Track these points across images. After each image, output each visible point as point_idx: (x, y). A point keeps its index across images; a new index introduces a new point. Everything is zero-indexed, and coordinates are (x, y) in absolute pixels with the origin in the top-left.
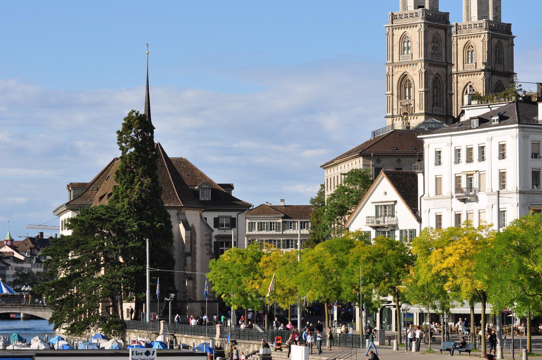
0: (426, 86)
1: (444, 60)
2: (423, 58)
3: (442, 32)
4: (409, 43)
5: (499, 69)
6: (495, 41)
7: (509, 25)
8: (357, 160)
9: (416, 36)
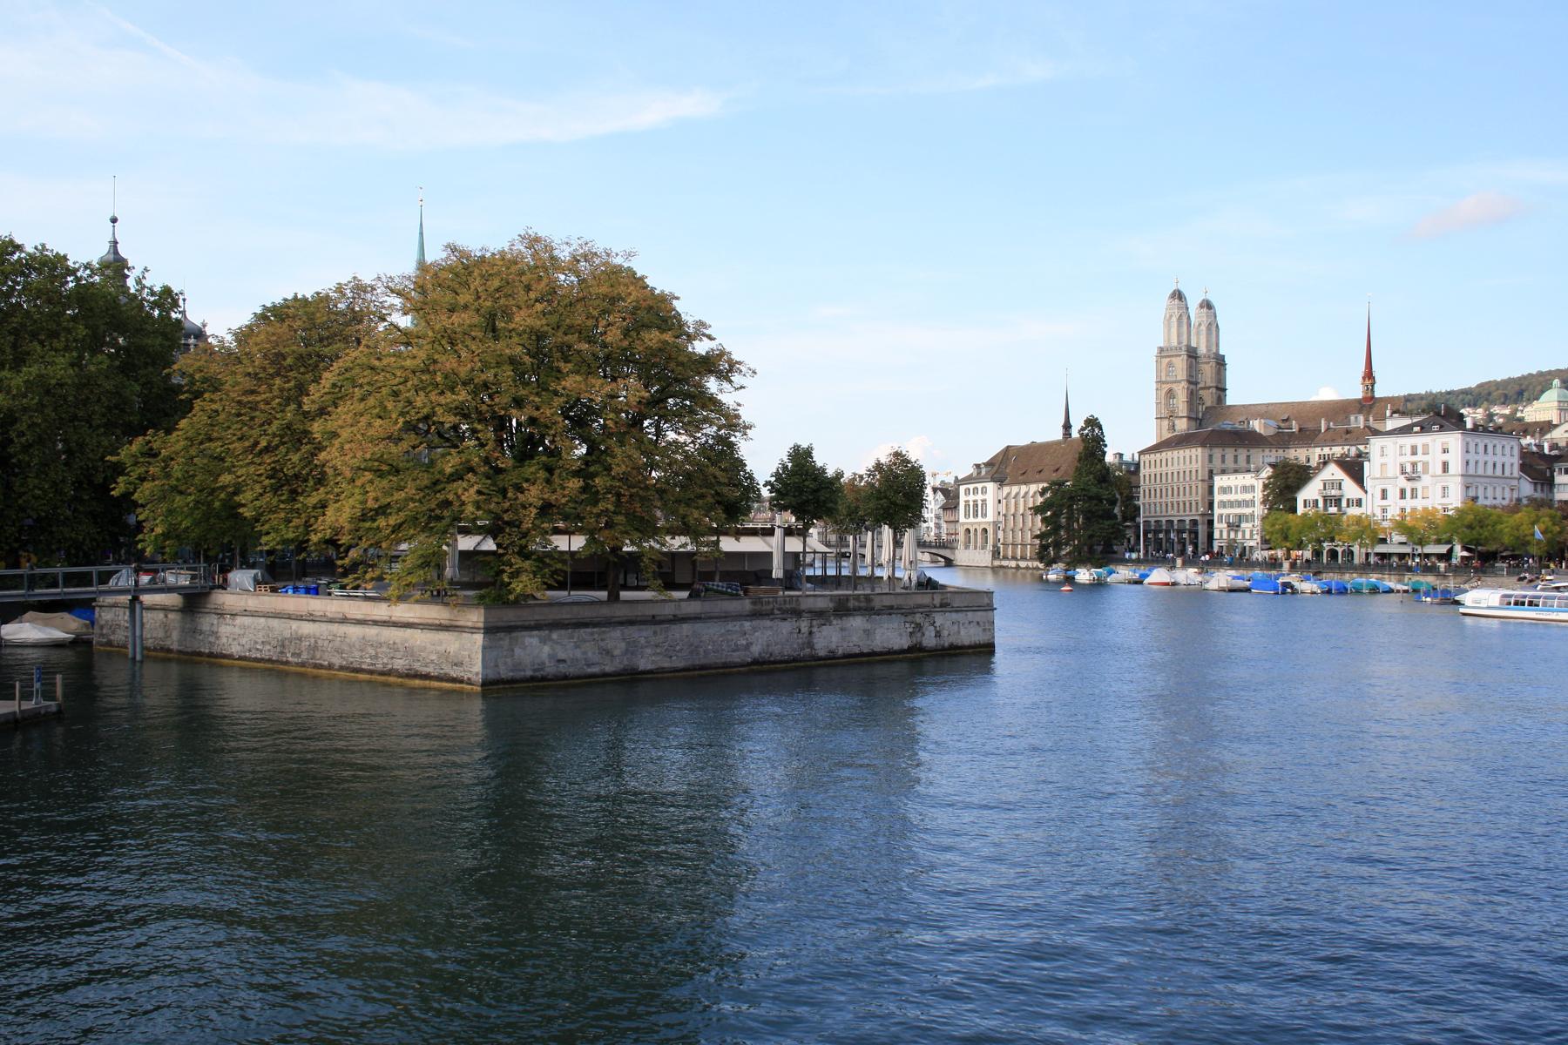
9: (1181, 364)
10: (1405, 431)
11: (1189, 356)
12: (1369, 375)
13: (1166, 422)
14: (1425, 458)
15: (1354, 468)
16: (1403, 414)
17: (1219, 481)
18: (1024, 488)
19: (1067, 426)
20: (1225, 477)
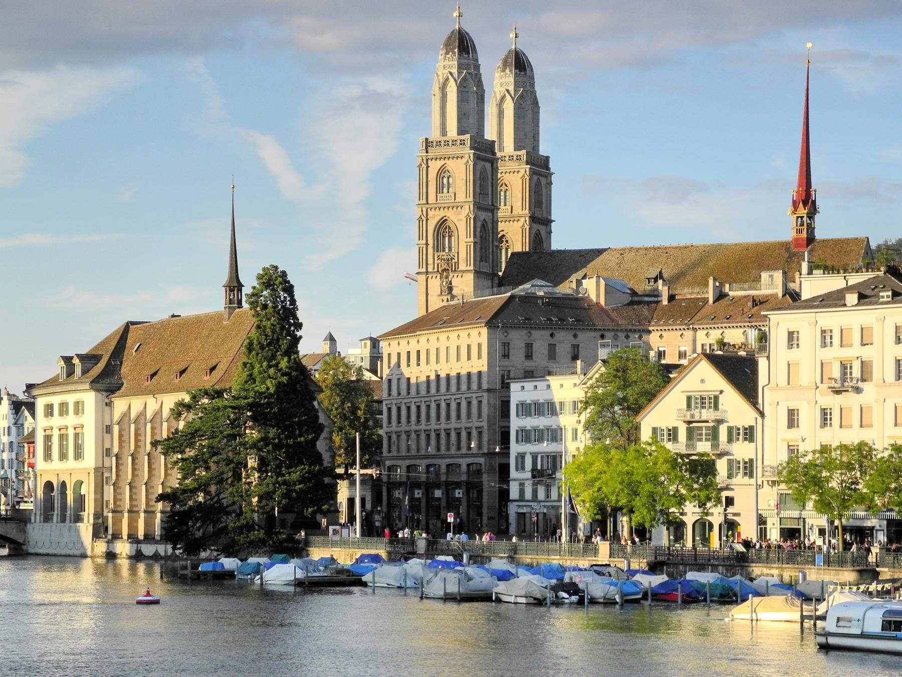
0: (475, 236)
1: (490, 203)
2: (471, 199)
3: (488, 166)
4: (451, 179)
5: (538, 214)
6: (535, 178)
7: (548, 158)
8: (474, 333)
9: (461, 170)
10: (833, 300)
11: (477, 158)
12: (806, 200)
13: (435, 283)
14: (867, 353)
15: (740, 371)
16: (829, 269)
17: (519, 393)
18: (152, 404)
19: (234, 286)
20: (529, 385)
